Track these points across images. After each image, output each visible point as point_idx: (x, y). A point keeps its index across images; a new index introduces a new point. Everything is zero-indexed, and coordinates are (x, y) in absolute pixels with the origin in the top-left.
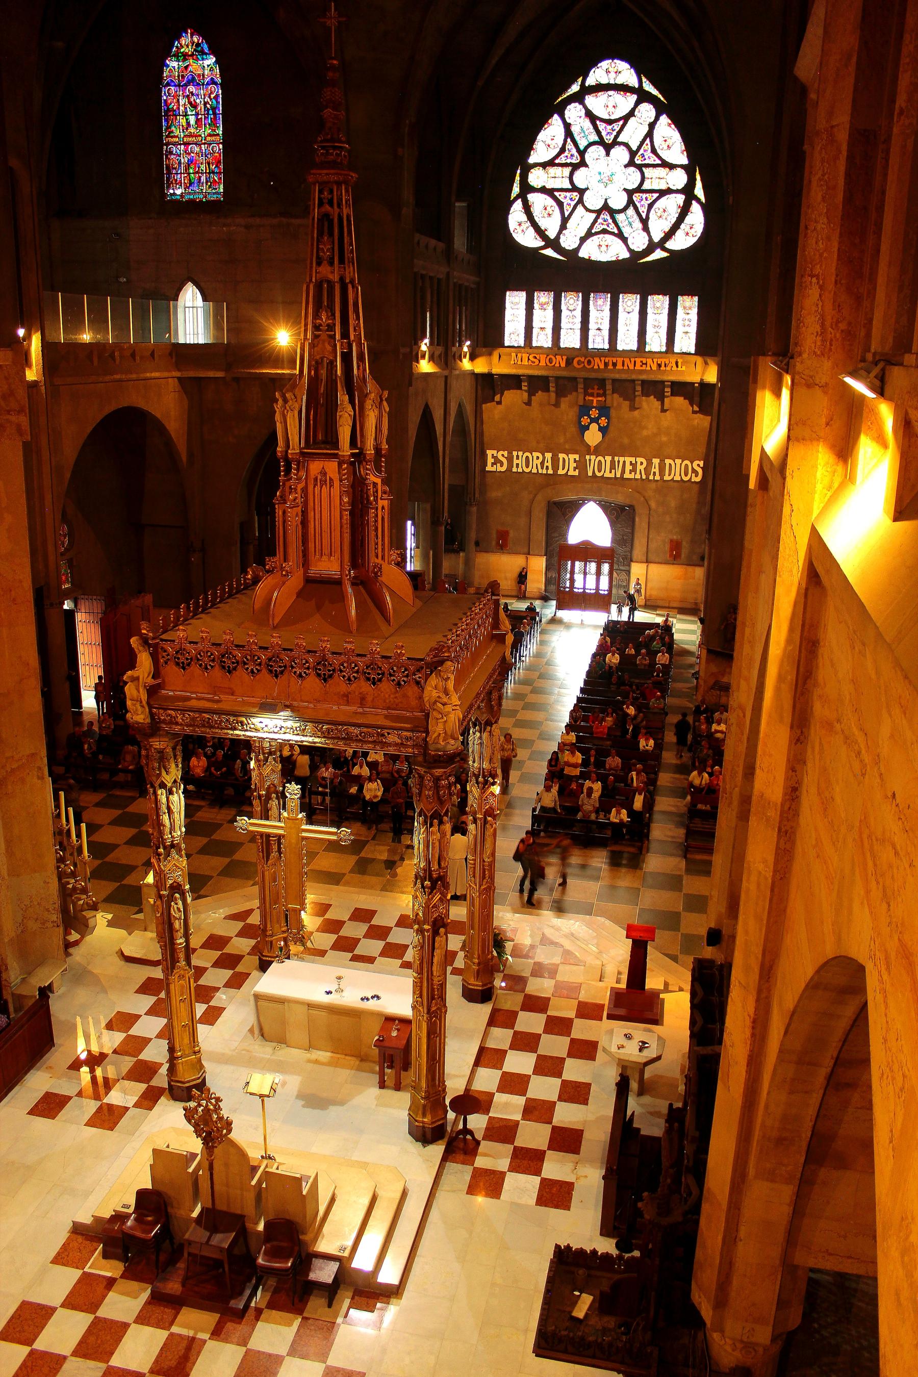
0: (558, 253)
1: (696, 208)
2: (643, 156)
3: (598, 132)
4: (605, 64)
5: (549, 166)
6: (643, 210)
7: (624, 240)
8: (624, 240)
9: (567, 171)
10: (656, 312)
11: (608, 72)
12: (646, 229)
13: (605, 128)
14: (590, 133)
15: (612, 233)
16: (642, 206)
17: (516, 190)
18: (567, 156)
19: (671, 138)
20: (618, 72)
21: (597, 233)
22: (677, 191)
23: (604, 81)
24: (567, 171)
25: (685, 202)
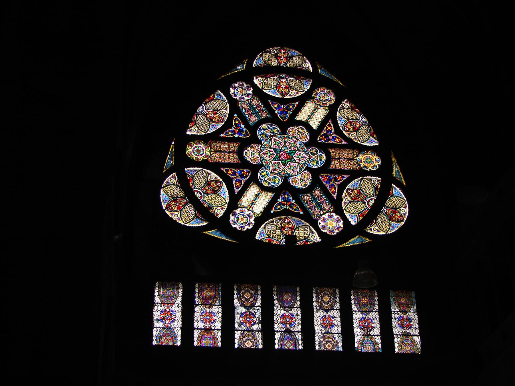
0: (227, 236)
1: (396, 190)
2: (326, 136)
3: (271, 111)
4: (273, 50)
5: (212, 140)
6: (334, 191)
7: (314, 223)
8: (314, 223)
9: (235, 147)
10: (363, 310)
11: (276, 56)
12: (339, 211)
13: (278, 106)
14: (261, 111)
15: (297, 215)
16: (332, 186)
17: (170, 161)
18: (234, 131)
19: (357, 120)
20: (288, 58)
21: (276, 215)
22: (371, 173)
23: (274, 63)
24: (235, 147)
25: (382, 184)
